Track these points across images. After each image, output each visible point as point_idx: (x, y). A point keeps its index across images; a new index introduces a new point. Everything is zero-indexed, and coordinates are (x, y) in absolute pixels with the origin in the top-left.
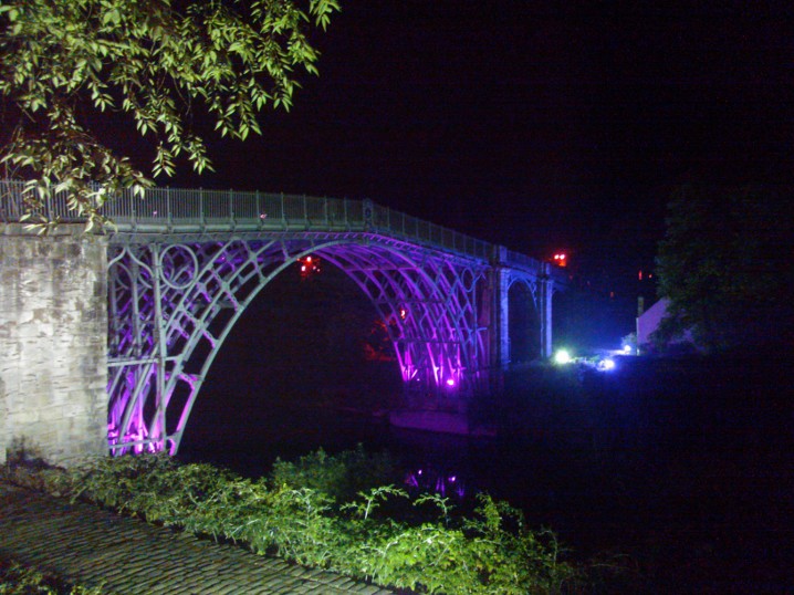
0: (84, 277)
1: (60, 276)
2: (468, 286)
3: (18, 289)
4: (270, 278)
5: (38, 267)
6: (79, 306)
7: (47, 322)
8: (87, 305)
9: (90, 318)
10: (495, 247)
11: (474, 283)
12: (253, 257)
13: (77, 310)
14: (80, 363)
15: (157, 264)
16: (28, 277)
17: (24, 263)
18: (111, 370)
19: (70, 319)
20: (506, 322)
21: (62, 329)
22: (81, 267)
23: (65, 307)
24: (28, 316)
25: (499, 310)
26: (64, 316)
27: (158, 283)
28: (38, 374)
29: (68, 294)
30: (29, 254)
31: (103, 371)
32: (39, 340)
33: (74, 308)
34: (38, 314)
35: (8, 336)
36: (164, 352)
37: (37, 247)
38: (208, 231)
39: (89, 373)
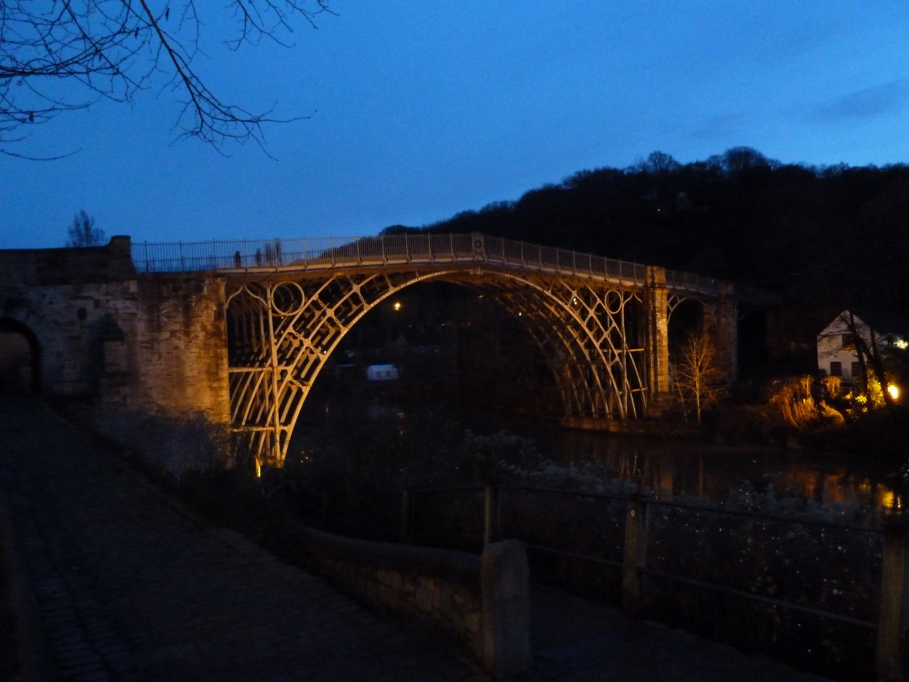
0: (207, 307)
1: (187, 309)
2: (614, 306)
3: (158, 317)
4: (372, 305)
5: (172, 301)
6: (204, 328)
7: (180, 339)
8: (209, 327)
9: (213, 336)
10: (649, 268)
11: (622, 305)
12: (356, 288)
13: (202, 331)
14: (205, 369)
15: (269, 296)
16: (165, 309)
17: (162, 299)
18: (231, 375)
19: (197, 337)
20: (665, 343)
21: (191, 344)
22: (204, 301)
23: (193, 328)
24: (166, 335)
25: (655, 331)
26: (193, 335)
27: (270, 312)
28: (174, 375)
29: (194, 319)
30: (165, 292)
31: (225, 375)
32: (174, 351)
33: (199, 329)
34: (173, 333)
35: (152, 348)
36: (275, 363)
37: (171, 287)
38: (309, 270)
39: (213, 374)
